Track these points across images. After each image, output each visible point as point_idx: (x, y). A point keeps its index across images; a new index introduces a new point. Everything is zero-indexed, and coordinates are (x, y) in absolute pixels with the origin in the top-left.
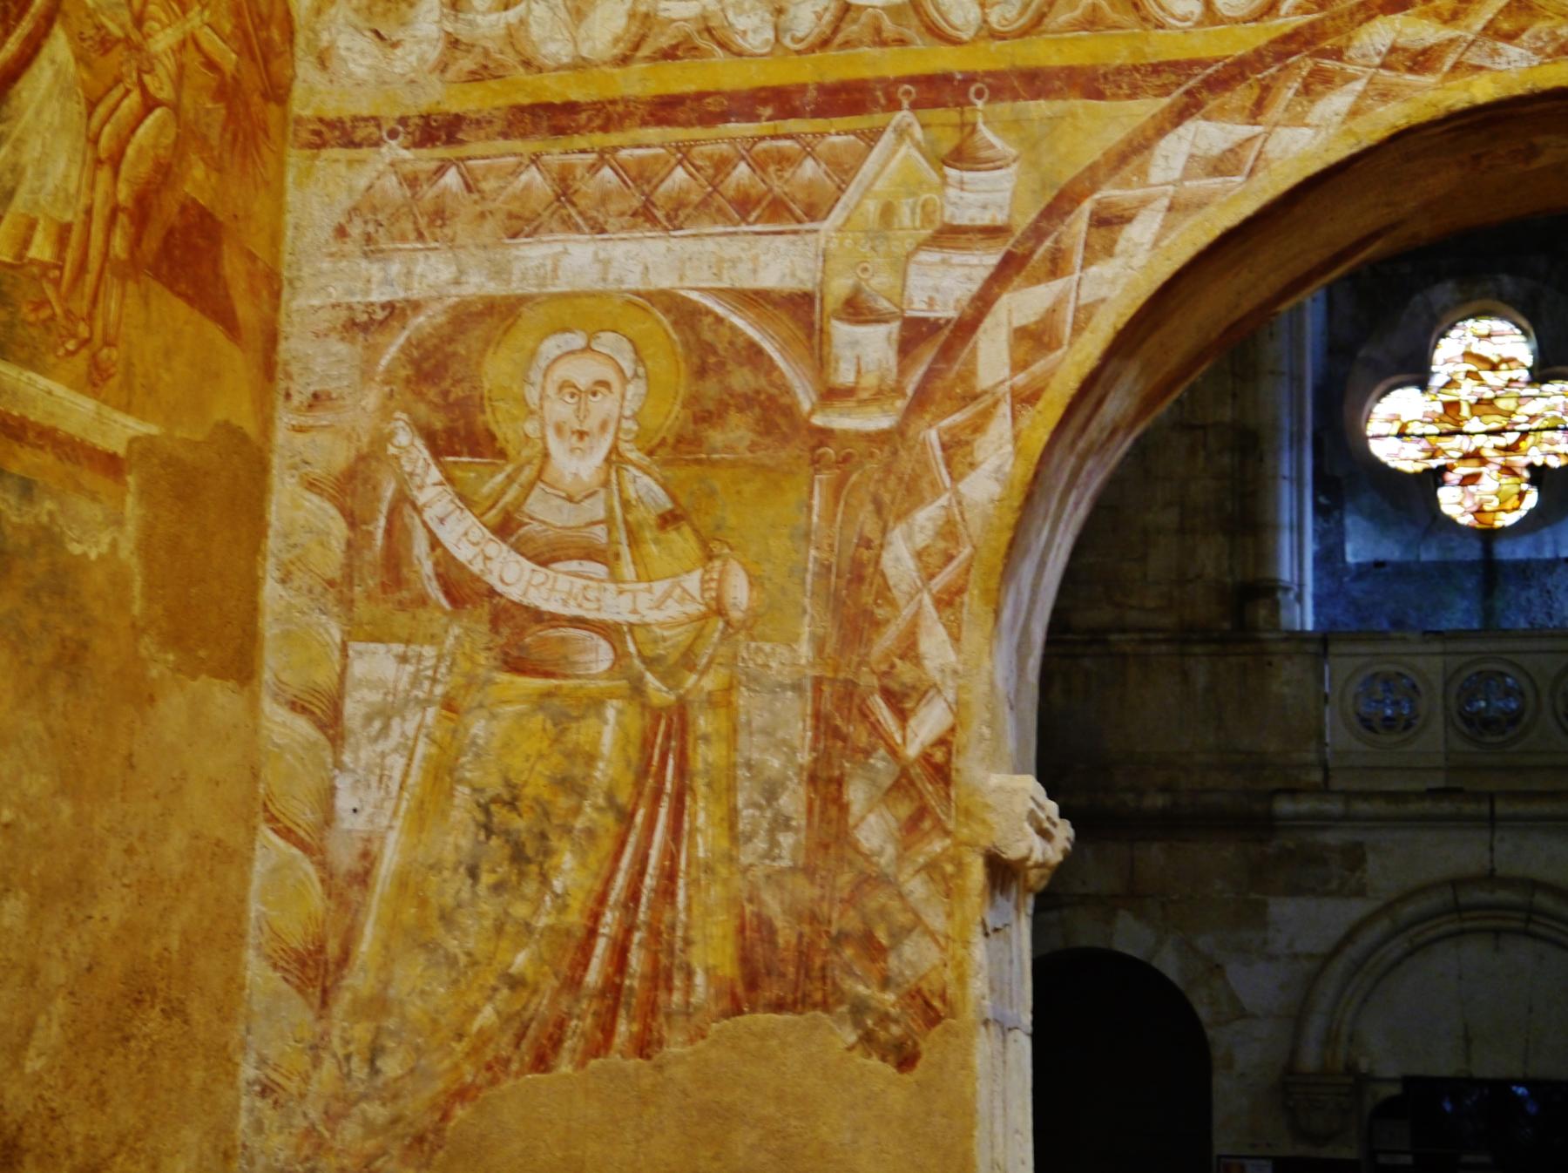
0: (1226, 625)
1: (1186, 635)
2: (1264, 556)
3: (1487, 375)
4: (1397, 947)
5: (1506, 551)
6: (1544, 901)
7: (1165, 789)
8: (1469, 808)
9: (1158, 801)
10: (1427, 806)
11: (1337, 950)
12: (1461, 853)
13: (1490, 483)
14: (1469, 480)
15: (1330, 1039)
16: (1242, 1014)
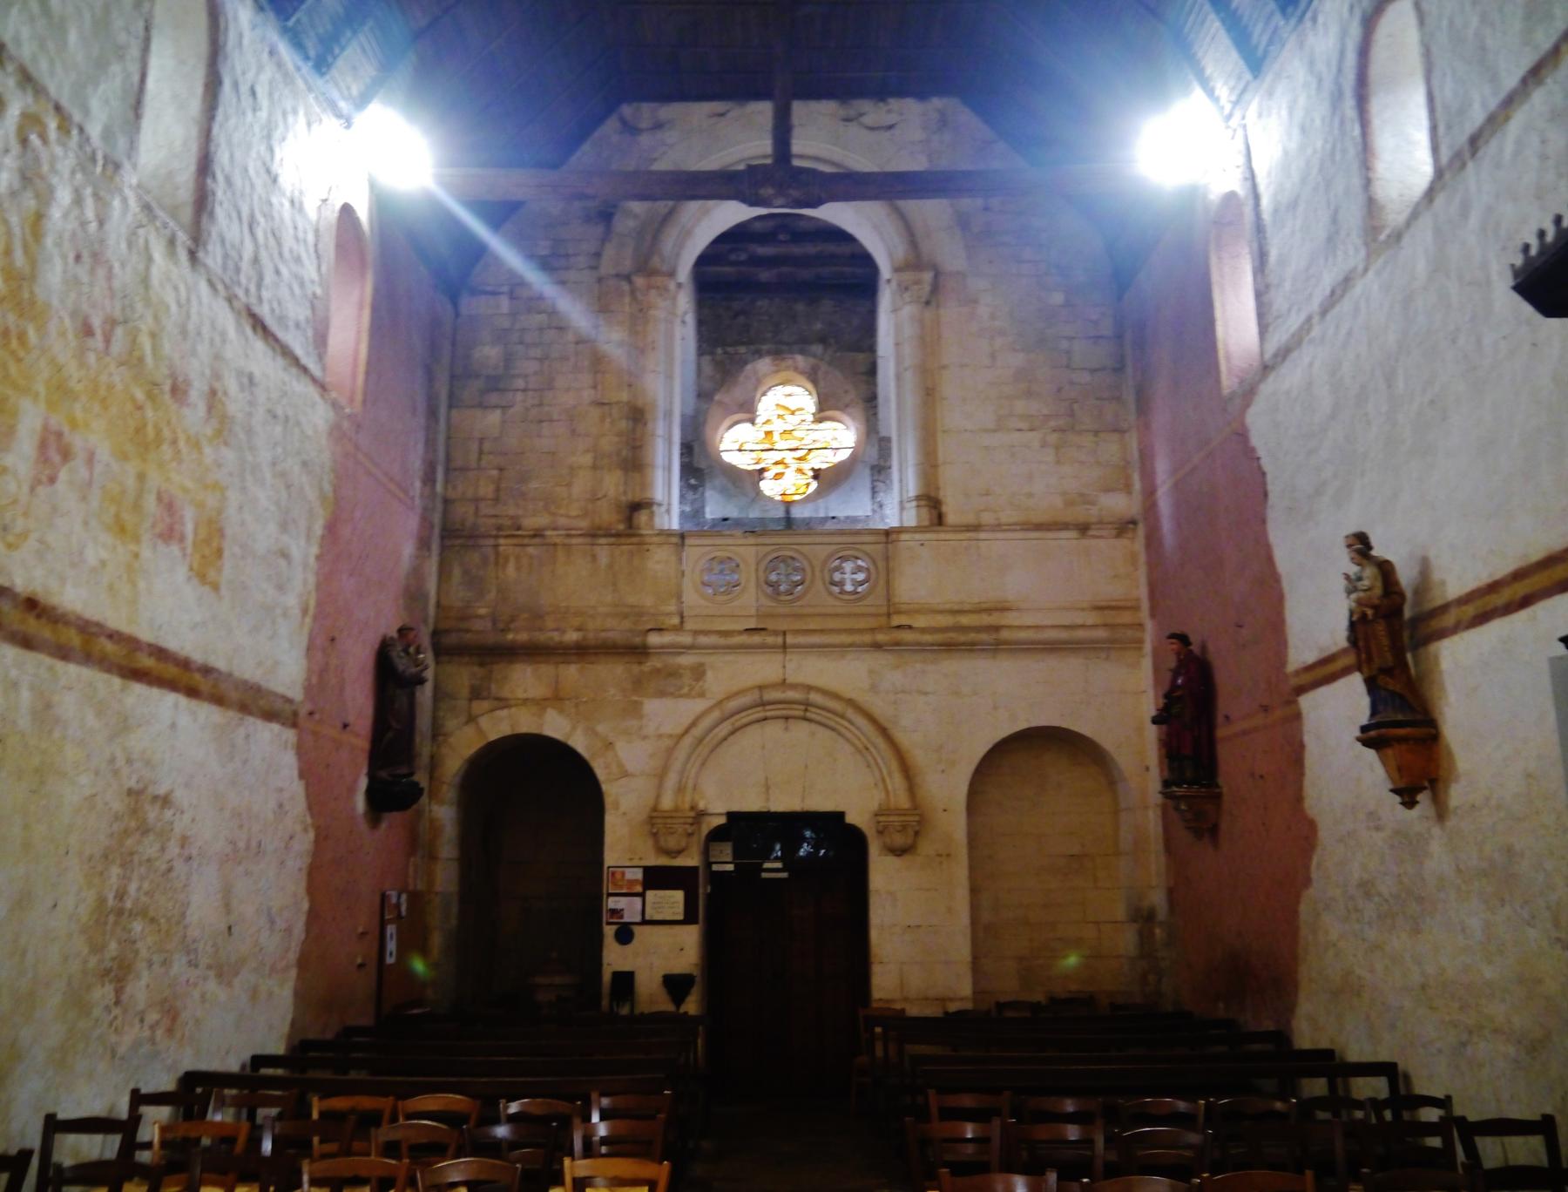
0: (621, 527)
1: (593, 534)
2: (645, 485)
3: (789, 418)
4: (726, 728)
5: (797, 513)
6: (815, 697)
7: (579, 629)
8: (770, 640)
9: (572, 636)
10: (743, 639)
11: (687, 731)
12: (763, 669)
13: (790, 475)
14: (778, 476)
15: (680, 790)
16: (625, 774)
